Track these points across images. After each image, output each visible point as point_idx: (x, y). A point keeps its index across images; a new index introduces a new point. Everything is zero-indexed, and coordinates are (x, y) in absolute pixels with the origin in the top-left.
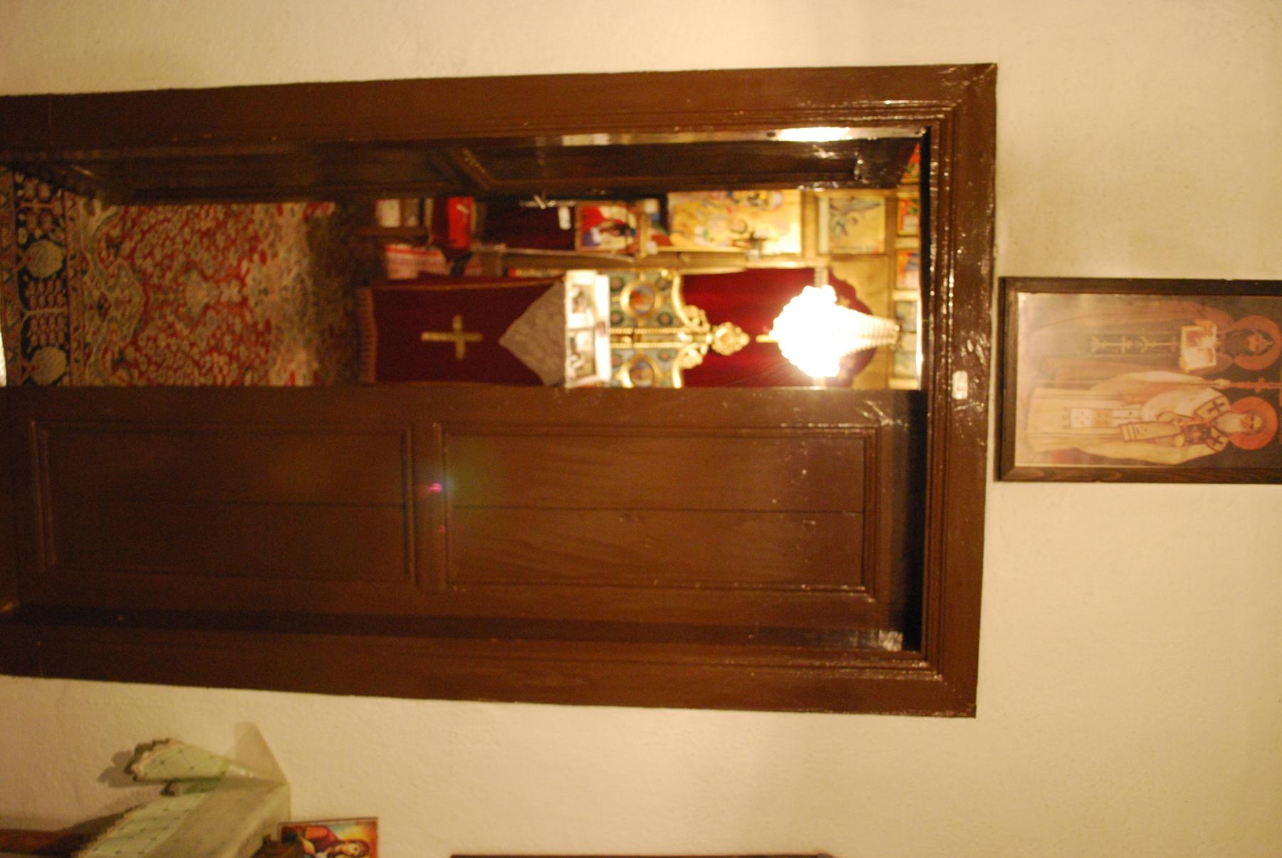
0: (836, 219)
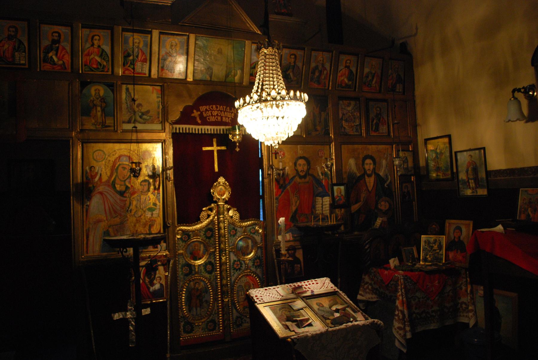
0: (138, 118)
